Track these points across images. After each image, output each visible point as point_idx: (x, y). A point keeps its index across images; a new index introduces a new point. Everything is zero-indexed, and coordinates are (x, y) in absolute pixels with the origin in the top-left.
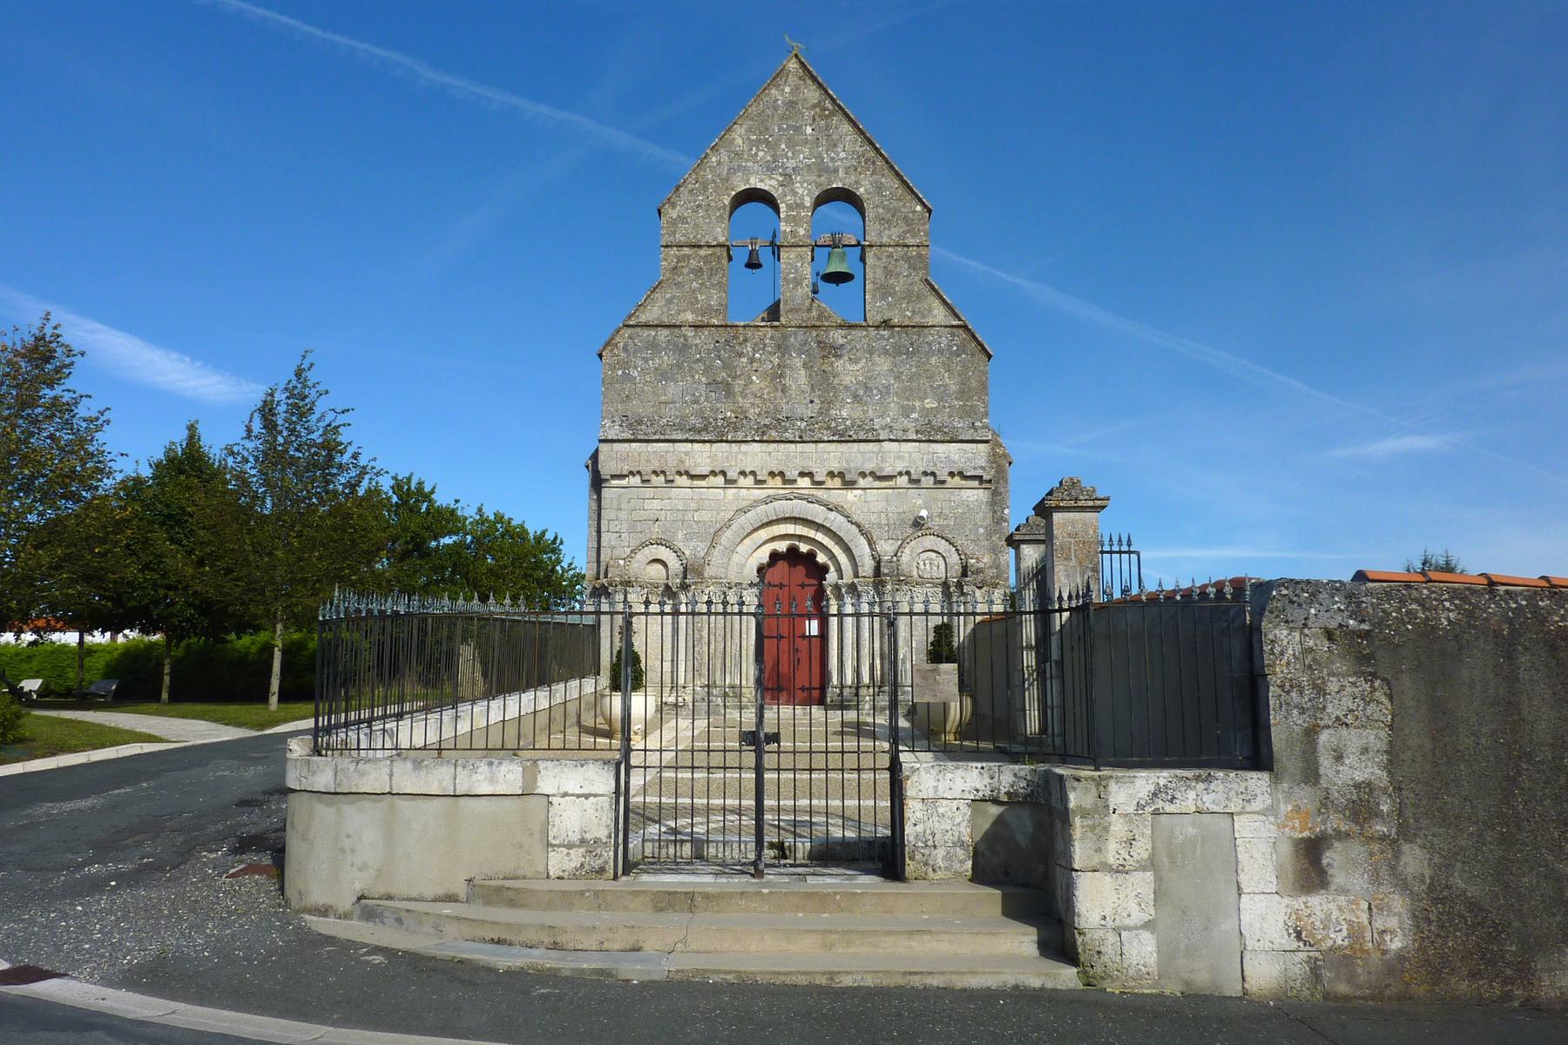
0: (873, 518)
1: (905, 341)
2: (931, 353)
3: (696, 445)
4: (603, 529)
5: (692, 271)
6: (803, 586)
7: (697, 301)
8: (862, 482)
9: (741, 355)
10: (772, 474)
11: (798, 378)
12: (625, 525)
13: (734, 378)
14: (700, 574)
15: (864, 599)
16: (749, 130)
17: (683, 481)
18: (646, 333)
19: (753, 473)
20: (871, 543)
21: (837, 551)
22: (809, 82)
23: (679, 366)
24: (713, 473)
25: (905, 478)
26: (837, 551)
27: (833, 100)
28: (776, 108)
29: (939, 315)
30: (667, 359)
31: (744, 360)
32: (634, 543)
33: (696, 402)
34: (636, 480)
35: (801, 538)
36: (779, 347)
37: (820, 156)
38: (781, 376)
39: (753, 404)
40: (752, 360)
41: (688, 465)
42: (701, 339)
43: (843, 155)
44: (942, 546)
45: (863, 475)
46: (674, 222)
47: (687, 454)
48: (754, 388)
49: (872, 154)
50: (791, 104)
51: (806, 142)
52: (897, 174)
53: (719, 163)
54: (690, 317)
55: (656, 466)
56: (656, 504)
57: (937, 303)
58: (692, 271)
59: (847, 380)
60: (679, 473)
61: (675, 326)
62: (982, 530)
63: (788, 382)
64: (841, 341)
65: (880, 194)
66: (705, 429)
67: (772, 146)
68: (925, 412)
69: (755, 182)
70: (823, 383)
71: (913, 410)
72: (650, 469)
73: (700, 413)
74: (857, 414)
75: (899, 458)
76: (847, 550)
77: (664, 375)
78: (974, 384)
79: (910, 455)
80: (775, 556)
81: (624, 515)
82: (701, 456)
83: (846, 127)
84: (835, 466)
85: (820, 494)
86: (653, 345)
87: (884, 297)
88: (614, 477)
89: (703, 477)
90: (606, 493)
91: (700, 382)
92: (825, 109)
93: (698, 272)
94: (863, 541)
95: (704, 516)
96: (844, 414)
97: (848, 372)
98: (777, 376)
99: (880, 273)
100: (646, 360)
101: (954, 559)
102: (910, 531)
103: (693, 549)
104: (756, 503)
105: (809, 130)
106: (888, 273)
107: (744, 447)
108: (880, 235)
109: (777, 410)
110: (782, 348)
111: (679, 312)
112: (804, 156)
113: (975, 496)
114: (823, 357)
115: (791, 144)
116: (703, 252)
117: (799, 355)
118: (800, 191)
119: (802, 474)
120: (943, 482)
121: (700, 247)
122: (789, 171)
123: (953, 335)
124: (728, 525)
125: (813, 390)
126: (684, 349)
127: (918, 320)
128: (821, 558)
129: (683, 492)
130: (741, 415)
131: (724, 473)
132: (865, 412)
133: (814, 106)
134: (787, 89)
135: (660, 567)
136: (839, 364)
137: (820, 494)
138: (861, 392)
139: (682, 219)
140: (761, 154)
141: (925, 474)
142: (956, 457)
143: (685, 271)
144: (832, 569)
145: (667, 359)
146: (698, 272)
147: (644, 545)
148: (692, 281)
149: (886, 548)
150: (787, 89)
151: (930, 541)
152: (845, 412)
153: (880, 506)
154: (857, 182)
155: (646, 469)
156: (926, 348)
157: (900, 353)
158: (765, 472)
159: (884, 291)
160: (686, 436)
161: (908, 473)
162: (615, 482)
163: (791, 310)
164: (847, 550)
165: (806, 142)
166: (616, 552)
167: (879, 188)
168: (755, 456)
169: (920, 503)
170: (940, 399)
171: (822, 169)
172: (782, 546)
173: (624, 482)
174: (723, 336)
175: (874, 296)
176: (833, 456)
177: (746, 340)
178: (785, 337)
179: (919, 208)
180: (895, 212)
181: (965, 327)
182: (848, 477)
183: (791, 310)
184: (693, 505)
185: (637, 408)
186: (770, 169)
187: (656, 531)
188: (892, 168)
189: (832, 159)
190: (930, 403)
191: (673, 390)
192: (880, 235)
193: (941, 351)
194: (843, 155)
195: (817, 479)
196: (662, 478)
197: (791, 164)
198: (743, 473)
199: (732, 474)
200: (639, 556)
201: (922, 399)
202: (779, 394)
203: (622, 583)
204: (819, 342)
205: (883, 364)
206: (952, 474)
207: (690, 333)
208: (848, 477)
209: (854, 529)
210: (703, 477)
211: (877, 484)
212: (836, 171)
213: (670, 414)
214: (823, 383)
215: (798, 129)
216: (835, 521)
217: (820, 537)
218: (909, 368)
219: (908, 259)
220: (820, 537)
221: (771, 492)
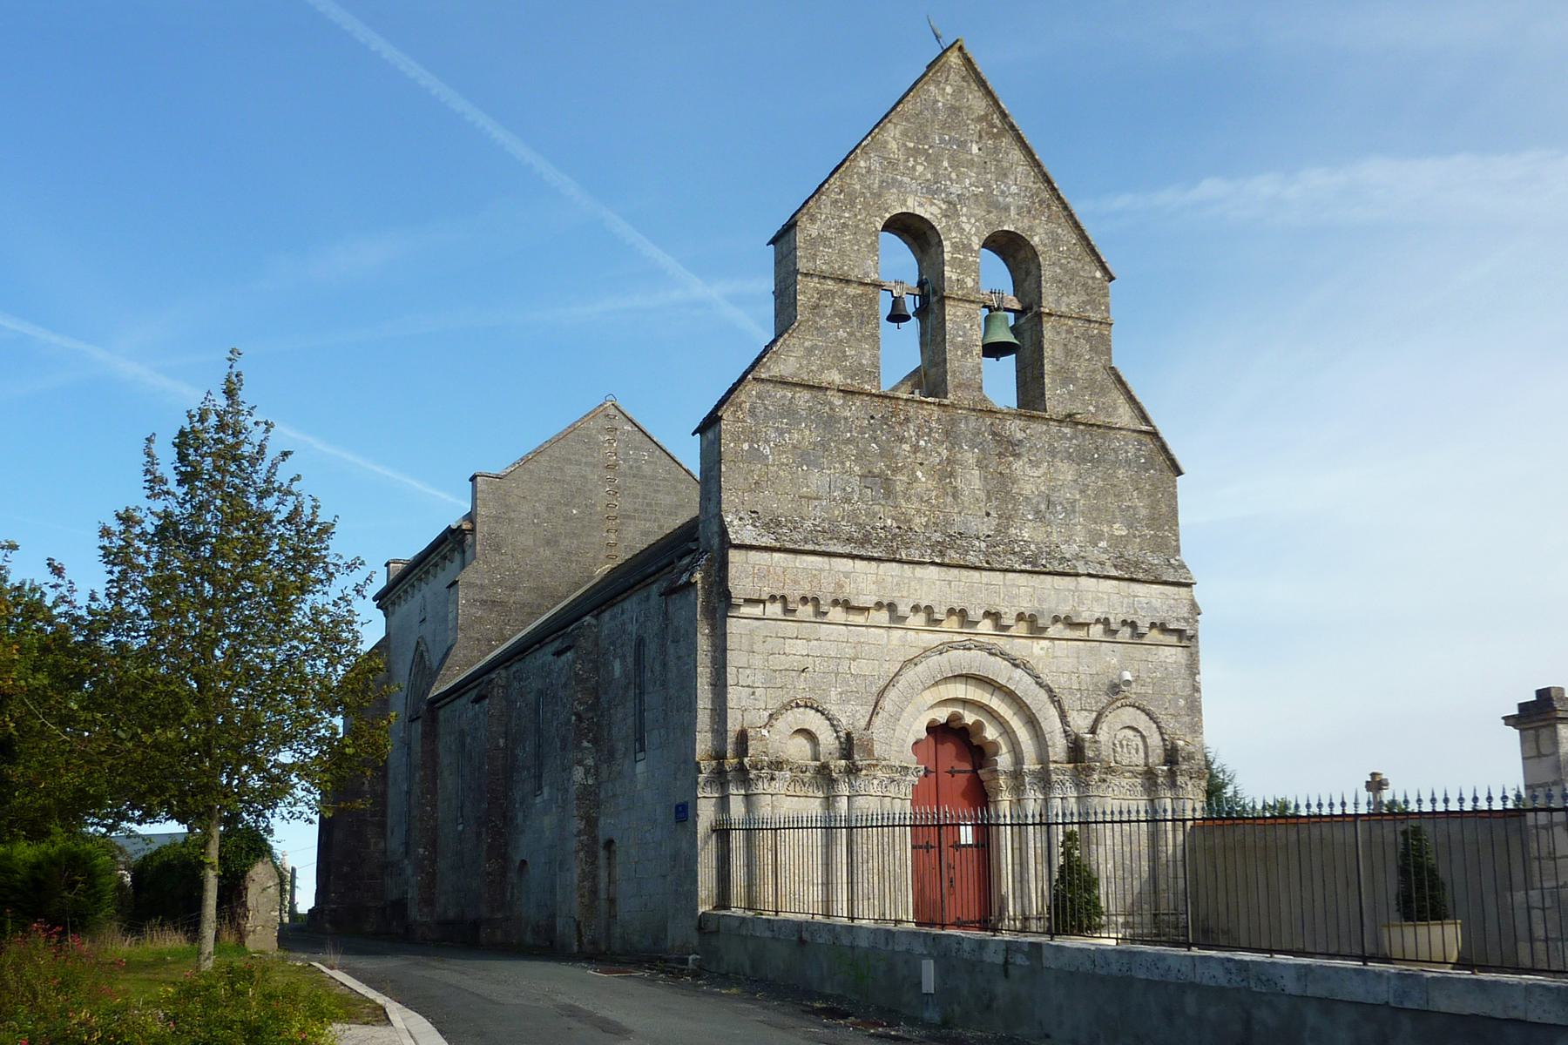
0: (1063, 679)
1: (1088, 444)
2: (1116, 464)
3: (858, 563)
4: (730, 680)
5: (837, 314)
6: (952, 773)
7: (845, 357)
8: (1052, 631)
9: (902, 440)
10: (951, 612)
11: (972, 481)
12: (759, 676)
13: (894, 472)
14: (869, 752)
15: (1057, 793)
16: (905, 134)
17: (837, 614)
18: (780, 392)
19: (929, 610)
20: (1063, 716)
21: (1016, 724)
22: (974, 86)
23: (824, 446)
24: (879, 605)
25: (1100, 627)
26: (1016, 724)
27: (1004, 115)
28: (935, 112)
29: (1124, 416)
30: (807, 435)
31: (906, 447)
32: (773, 705)
33: (848, 500)
34: (775, 609)
35: (965, 702)
36: (947, 433)
37: (987, 186)
38: (951, 475)
39: (918, 511)
40: (916, 449)
41: (848, 592)
42: (851, 411)
43: (1014, 189)
44: (1142, 722)
45: (1056, 619)
46: (813, 242)
47: (847, 575)
48: (919, 488)
49: (1046, 195)
50: (954, 110)
51: (971, 163)
52: (1077, 226)
53: (869, 171)
54: (836, 377)
55: (806, 589)
56: (800, 647)
57: (1121, 400)
58: (837, 314)
59: (1028, 489)
60: (836, 603)
61: (820, 388)
62: (1182, 702)
63: (959, 483)
64: (1020, 435)
65: (1056, 247)
66: (866, 540)
67: (933, 161)
68: (1116, 541)
69: (914, 206)
70: (1001, 489)
71: (1101, 536)
72: (798, 594)
73: (852, 517)
74: (1040, 536)
75: (1098, 600)
76: (1032, 722)
77: (806, 457)
78: (1164, 510)
79: (1102, 598)
80: (933, 729)
81: (757, 661)
82: (867, 580)
83: (1017, 155)
84: (1026, 607)
85: (1003, 643)
86: (789, 412)
87: (1065, 382)
88: (748, 601)
89: (863, 610)
90: (733, 626)
91: (851, 473)
92: (993, 126)
93: (845, 316)
94: (1053, 713)
95: (863, 667)
96: (1026, 535)
97: (1029, 477)
98: (946, 473)
99: (1059, 353)
100: (781, 432)
101: (1155, 740)
102: (1105, 699)
103: (852, 716)
104: (927, 652)
105: (975, 149)
106: (1068, 353)
107: (919, 570)
108: (1058, 301)
109: (948, 523)
110: (950, 436)
111: (822, 369)
112: (968, 183)
113: (1173, 655)
114: (1000, 455)
115: (955, 164)
116: (852, 290)
117: (972, 447)
118: (967, 227)
119: (987, 614)
120: (1142, 635)
121: (848, 282)
122: (954, 198)
123: (1140, 443)
124: (891, 683)
125: (989, 499)
126: (829, 422)
127: (1102, 419)
128: (991, 733)
129: (836, 632)
130: (904, 522)
131: (891, 607)
132: (1049, 534)
133: (980, 119)
134: (949, 90)
135: (801, 741)
136: (1018, 465)
137: (1003, 643)
138: (1043, 507)
139: (823, 239)
140: (920, 168)
141: (1124, 623)
142: (1156, 603)
143: (829, 312)
144: (1004, 749)
145: (807, 435)
146: (845, 316)
147: (787, 707)
148: (838, 328)
149: (1080, 722)
150: (949, 90)
151: (1129, 715)
152: (1027, 532)
153: (1069, 664)
154: (1031, 228)
155: (794, 594)
156: (1112, 457)
157: (1084, 460)
158: (944, 609)
159: (1066, 377)
160: (848, 549)
161: (1106, 622)
162: (746, 610)
163: (959, 386)
164: (1032, 722)
165: (971, 163)
166: (748, 716)
167: (1056, 240)
168: (931, 585)
169: (1113, 659)
170: (1130, 526)
171: (993, 205)
172: (942, 715)
173: (757, 611)
174: (880, 409)
175: (1054, 381)
176: (1020, 593)
177: (907, 420)
178: (954, 422)
179: (1098, 274)
180: (1073, 274)
181: (1154, 435)
182: (1041, 623)
183: (959, 386)
184: (850, 652)
185: (781, 505)
186: (931, 191)
187: (801, 688)
188: (1071, 216)
189: (1003, 192)
190: (1120, 530)
191: (816, 480)
192: (1058, 301)
193: (1128, 462)
194: (1014, 189)
195: (1005, 622)
196: (809, 608)
197: (956, 189)
198: (916, 609)
199: (904, 609)
200: (779, 724)
201: (1111, 523)
202: (949, 499)
203: (771, 765)
204: (994, 434)
205: (1067, 472)
206: (1153, 625)
207: (838, 401)
208: (1041, 623)
209: (1043, 695)
210: (863, 610)
211: (1069, 633)
212: (1007, 209)
213: (814, 514)
214: (1001, 489)
215: (962, 145)
216: (1020, 682)
217: (995, 703)
218: (1094, 481)
219: (1089, 339)
220: (995, 703)
221: (946, 637)
